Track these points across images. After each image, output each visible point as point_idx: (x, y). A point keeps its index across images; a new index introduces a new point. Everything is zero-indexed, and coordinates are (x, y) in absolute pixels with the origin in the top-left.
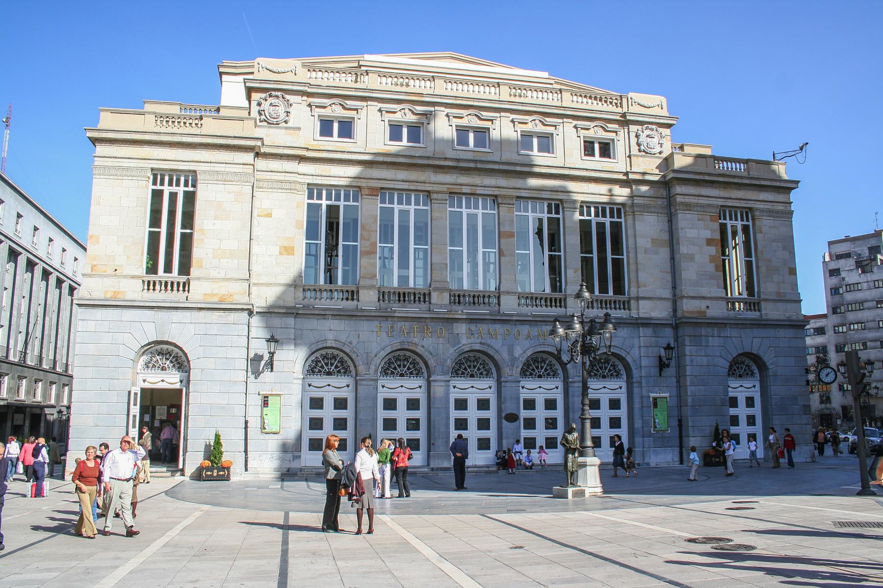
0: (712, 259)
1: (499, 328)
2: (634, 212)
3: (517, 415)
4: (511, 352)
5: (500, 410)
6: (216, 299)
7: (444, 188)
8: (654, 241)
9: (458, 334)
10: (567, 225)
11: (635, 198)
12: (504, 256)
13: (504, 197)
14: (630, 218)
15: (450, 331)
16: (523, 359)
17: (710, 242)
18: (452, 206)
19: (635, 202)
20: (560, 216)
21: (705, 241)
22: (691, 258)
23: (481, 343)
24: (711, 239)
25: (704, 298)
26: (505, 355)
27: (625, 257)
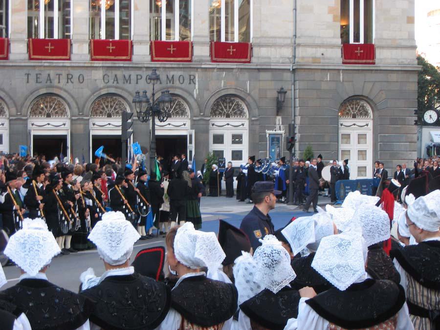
1: (133, 74)
9: (96, 80)
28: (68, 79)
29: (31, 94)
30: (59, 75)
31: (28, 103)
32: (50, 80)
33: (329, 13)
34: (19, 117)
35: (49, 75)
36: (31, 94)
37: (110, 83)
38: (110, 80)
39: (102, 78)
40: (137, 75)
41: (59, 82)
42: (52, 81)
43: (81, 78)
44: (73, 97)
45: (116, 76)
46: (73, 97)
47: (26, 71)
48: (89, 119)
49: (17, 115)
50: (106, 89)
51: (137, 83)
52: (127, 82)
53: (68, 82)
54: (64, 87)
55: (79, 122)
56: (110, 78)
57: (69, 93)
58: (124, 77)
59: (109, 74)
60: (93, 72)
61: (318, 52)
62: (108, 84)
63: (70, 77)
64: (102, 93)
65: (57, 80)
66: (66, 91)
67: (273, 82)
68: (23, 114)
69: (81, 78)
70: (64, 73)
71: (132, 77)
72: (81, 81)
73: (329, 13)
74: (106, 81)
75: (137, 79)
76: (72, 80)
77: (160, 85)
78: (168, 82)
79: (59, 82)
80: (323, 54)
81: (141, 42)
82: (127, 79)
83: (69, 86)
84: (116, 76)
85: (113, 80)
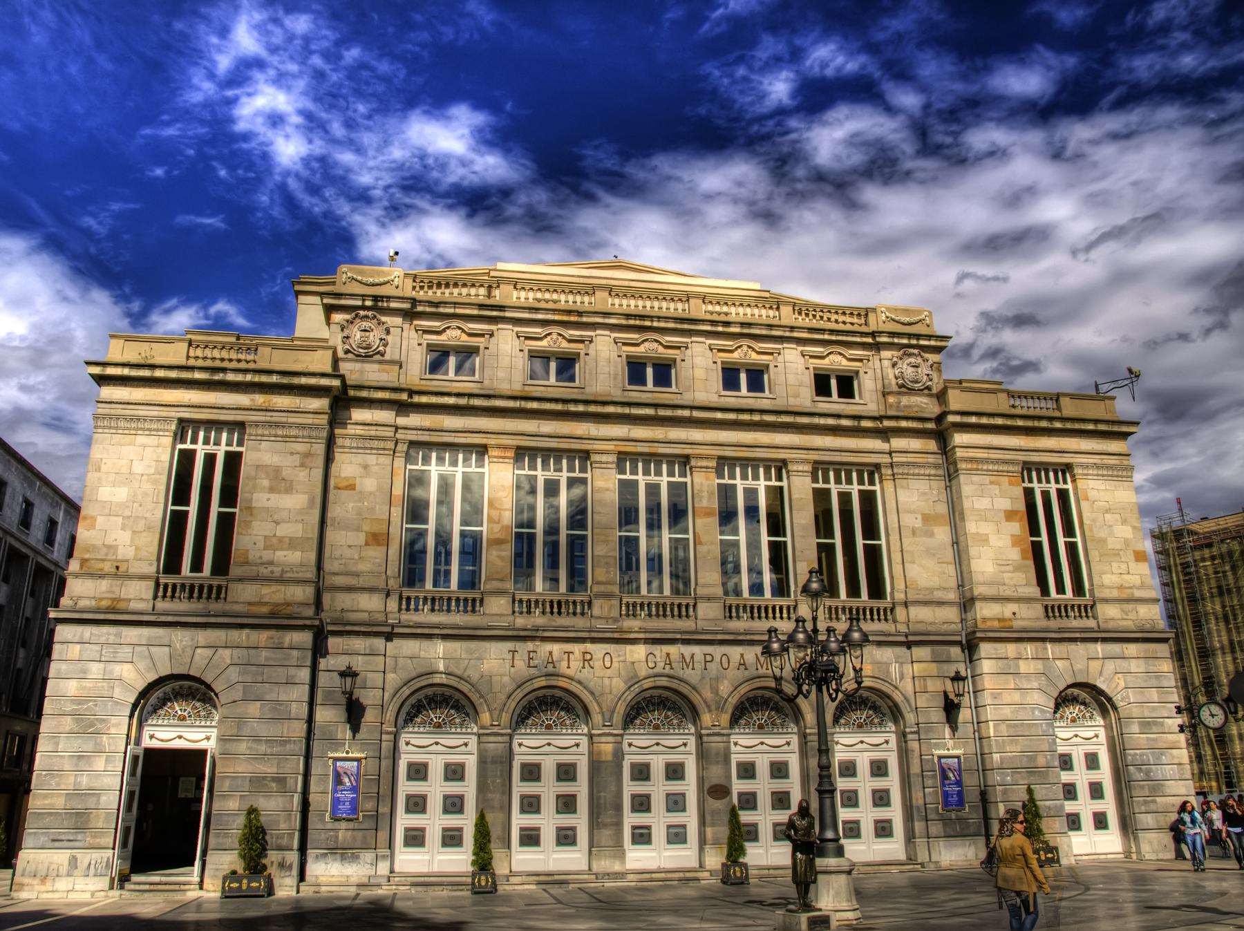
0: (1016, 541)
2: (893, 475)
3: (726, 787)
4: (715, 691)
5: (701, 780)
6: (265, 610)
7: (609, 446)
8: (927, 518)
9: (633, 663)
10: (795, 496)
11: (893, 455)
12: (701, 544)
13: (700, 457)
14: (889, 486)
15: (622, 659)
16: (733, 701)
17: (1010, 515)
18: (622, 471)
19: (894, 460)
20: (784, 484)
21: (1002, 515)
22: (984, 540)
23: (669, 676)
24: (1012, 511)
25: (1008, 600)
26: (708, 694)
27: (883, 542)
28: (584, 660)
29: (519, 687)
30: (569, 653)
31: (512, 704)
32: (553, 662)
33: (1014, 545)
34: (495, 730)
35: (551, 653)
36: (519, 687)
37: (659, 670)
38: (658, 664)
39: (644, 659)
40: (705, 655)
41: (569, 667)
42: (557, 665)
43: (607, 658)
44: (592, 693)
45: (668, 655)
46: (592, 693)
47: (509, 645)
48: (622, 735)
49: (492, 725)
50: (652, 679)
51: (706, 669)
52: (688, 667)
53: (584, 668)
54: (578, 676)
55: (604, 739)
56: (658, 659)
57: (585, 688)
58: (683, 657)
59: (657, 653)
60: (629, 647)
61: (1008, 610)
62: (656, 671)
63: (588, 657)
64: (645, 686)
65: (565, 664)
66: (580, 682)
67: (934, 665)
68: (502, 724)
69: (607, 658)
70: (577, 648)
71: (696, 659)
72: (608, 664)
73: (1014, 545)
74: (651, 665)
75: (706, 662)
76: (591, 662)
77: (747, 672)
78: (759, 667)
79: (569, 667)
80: (1014, 614)
81: (709, 599)
82: (688, 661)
83: (586, 674)
84: (668, 655)
85: (663, 664)
